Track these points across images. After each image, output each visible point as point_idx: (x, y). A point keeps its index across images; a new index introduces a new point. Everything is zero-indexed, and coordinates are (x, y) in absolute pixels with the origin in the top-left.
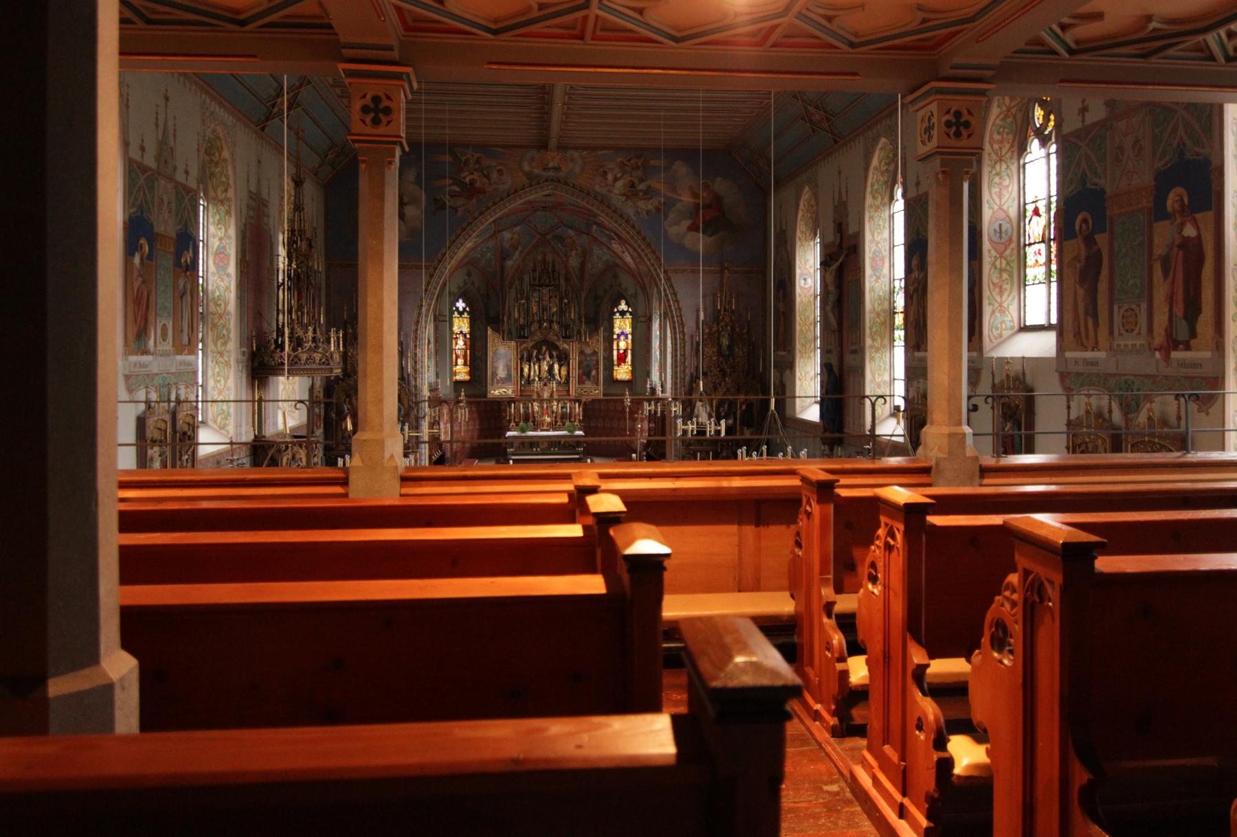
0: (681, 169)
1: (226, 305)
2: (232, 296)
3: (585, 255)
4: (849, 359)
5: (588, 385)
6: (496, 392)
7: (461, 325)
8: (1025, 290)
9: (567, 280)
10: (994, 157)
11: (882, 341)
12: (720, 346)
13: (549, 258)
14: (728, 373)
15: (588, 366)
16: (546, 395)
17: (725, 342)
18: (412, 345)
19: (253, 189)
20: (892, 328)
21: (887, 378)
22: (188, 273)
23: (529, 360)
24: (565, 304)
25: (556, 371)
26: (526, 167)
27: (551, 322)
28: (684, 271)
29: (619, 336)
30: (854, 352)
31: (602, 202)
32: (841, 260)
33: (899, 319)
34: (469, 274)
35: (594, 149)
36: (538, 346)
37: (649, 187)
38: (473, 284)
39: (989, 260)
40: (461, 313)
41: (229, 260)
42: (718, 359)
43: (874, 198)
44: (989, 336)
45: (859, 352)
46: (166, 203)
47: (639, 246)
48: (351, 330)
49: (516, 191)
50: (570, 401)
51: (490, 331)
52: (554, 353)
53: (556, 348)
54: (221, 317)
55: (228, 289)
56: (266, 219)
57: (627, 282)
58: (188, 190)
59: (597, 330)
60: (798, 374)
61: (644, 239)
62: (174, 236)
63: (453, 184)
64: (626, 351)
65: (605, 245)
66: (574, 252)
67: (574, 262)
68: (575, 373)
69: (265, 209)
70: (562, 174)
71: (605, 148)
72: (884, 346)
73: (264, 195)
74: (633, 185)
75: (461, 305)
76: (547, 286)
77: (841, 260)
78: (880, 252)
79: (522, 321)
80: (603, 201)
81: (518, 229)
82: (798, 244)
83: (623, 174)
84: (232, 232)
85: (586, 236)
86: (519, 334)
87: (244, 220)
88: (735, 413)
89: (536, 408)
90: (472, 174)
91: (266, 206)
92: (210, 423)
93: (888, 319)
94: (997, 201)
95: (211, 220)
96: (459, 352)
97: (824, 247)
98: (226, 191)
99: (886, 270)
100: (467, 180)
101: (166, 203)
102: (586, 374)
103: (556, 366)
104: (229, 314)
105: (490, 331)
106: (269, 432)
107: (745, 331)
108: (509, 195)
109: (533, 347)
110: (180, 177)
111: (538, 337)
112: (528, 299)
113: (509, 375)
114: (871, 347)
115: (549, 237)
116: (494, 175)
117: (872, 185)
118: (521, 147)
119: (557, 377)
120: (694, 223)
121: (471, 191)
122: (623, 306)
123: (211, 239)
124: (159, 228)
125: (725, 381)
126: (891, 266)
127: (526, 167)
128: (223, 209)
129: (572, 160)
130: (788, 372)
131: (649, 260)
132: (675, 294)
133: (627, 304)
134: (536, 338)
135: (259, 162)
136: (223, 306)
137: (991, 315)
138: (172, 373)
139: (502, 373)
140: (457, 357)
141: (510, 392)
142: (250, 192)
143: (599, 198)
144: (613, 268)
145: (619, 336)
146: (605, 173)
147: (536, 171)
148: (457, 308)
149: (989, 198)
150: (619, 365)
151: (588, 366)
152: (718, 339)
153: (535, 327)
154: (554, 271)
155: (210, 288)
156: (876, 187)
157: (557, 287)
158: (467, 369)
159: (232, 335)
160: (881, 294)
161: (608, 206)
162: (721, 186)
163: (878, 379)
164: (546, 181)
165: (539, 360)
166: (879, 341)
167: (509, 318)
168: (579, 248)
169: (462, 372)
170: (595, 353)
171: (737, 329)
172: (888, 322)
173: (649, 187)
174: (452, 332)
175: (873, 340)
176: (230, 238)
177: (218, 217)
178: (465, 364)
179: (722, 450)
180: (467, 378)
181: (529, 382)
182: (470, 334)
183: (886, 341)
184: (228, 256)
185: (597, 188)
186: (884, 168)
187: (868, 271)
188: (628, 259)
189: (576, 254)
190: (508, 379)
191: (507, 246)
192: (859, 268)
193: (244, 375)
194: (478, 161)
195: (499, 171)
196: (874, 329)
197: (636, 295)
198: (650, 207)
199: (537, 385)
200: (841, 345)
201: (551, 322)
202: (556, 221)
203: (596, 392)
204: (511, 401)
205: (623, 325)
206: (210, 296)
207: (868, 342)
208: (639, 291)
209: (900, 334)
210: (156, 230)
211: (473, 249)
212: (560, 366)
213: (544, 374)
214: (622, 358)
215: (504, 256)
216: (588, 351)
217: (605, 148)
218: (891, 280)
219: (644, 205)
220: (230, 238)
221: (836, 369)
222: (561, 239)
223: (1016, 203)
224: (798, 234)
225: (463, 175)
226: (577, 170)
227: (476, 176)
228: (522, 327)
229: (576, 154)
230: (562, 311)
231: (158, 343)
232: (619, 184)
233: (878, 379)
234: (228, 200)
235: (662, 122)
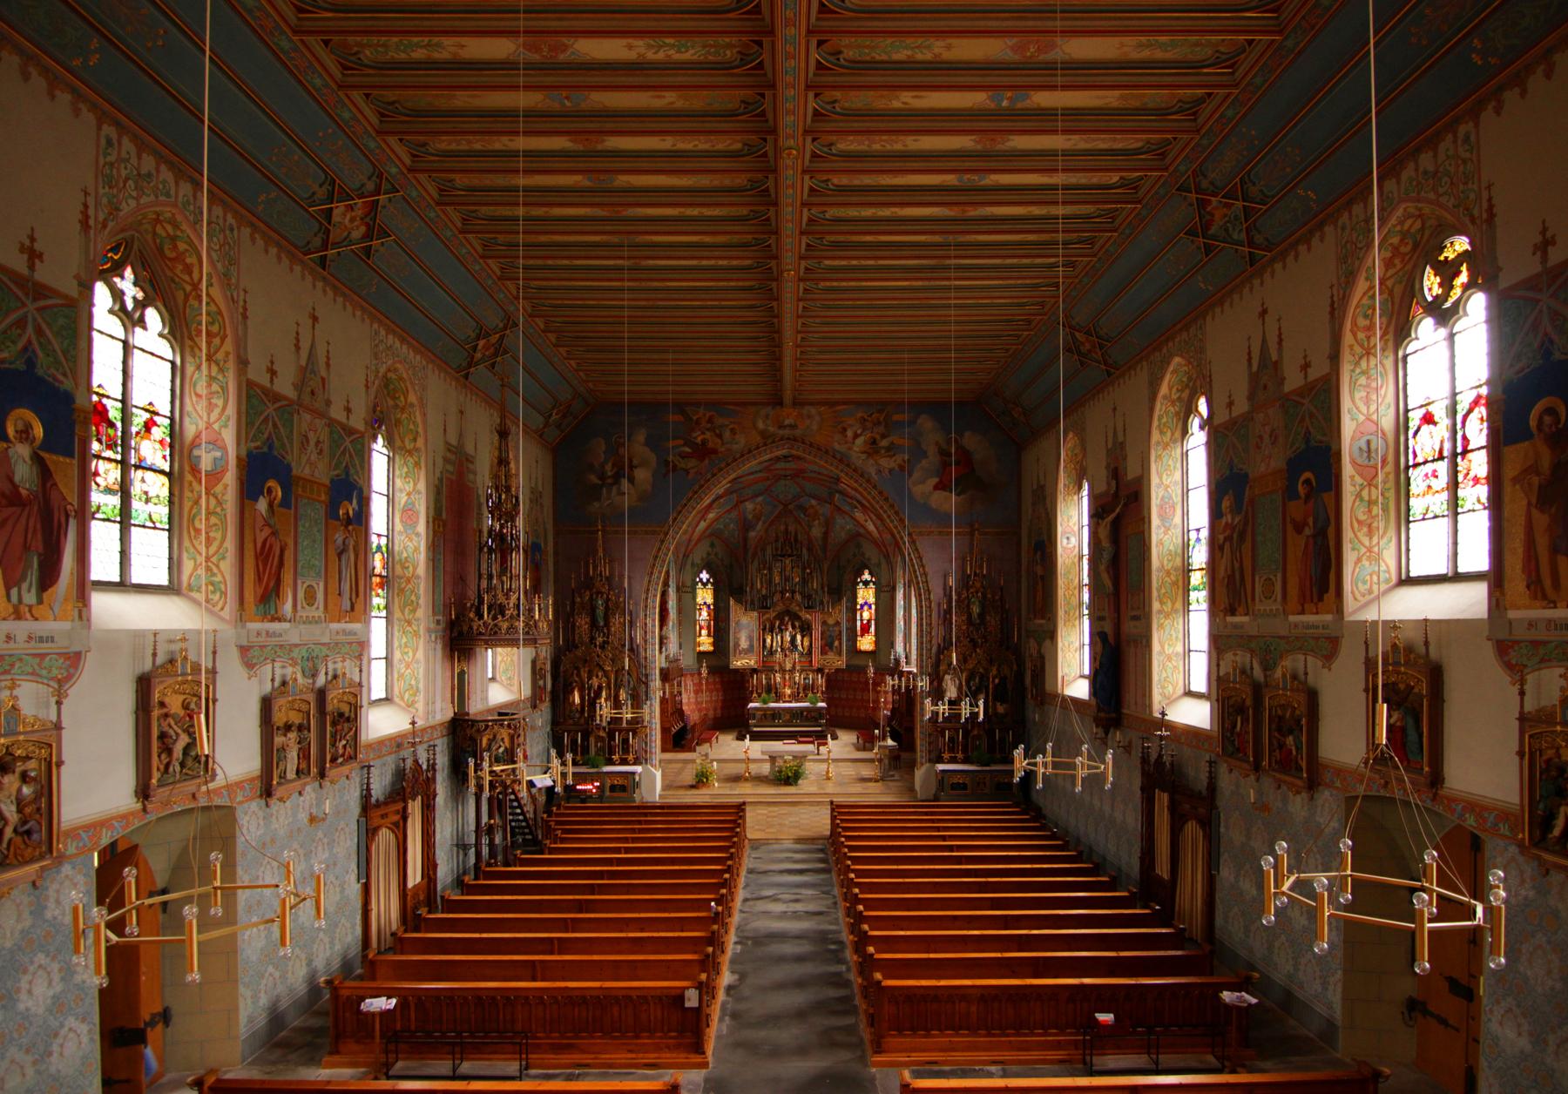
0: (926, 423)
1: (415, 568)
2: (422, 557)
3: (828, 525)
4: (1129, 627)
5: (831, 656)
6: (738, 663)
7: (705, 596)
8: (1408, 529)
9: (809, 550)
10: (1358, 350)
11: (1173, 604)
12: (970, 615)
13: (791, 528)
16: (788, 666)
17: (976, 609)
18: (642, 615)
19: (454, 442)
20: (1186, 590)
21: (1179, 648)
22: (350, 528)
23: (772, 631)
25: (799, 642)
26: (761, 425)
27: (793, 592)
28: (929, 533)
29: (862, 606)
30: (1136, 618)
31: (841, 461)
32: (1118, 510)
33: (1197, 578)
34: (712, 545)
35: (831, 404)
36: (780, 617)
37: (892, 443)
38: (716, 554)
39: (1352, 489)
40: (704, 585)
41: (418, 518)
43: (1162, 433)
44: (1353, 592)
45: (1143, 618)
46: (312, 443)
47: (882, 507)
48: (578, 600)
49: (750, 451)
50: (813, 671)
51: (732, 602)
52: (797, 624)
53: (799, 618)
54: (409, 581)
55: (416, 549)
56: (471, 477)
57: (871, 553)
58: (351, 431)
59: (840, 599)
60: (1060, 645)
61: (886, 499)
62: (327, 482)
63: (685, 445)
64: (869, 621)
67: (817, 532)
68: (817, 644)
69: (470, 466)
70: (798, 432)
71: (844, 403)
72: (1176, 611)
73: (470, 449)
74: (874, 442)
75: (704, 576)
77: (1118, 510)
78: (1171, 498)
79: (764, 592)
80: (843, 460)
81: (760, 499)
82: (1060, 498)
83: (864, 430)
84: (422, 486)
86: (762, 605)
87: (438, 474)
88: (987, 688)
89: (778, 679)
90: (703, 433)
91: (472, 462)
92: (397, 700)
93: (1180, 578)
94: (1364, 409)
95: (397, 473)
96: (703, 623)
97: (1093, 497)
98: (415, 440)
99: (1177, 520)
100: (699, 440)
101: (312, 443)
102: (827, 646)
103: (799, 637)
104: (418, 577)
105: (732, 602)
106: (475, 707)
108: (742, 456)
109: (775, 618)
110: (337, 413)
111: (780, 607)
112: (770, 569)
113: (751, 646)
114: (1160, 612)
115: (791, 507)
116: (727, 434)
117: (1159, 420)
118: (755, 404)
119: (800, 648)
120: (941, 482)
121: (703, 452)
122: (867, 576)
123: (398, 494)
124: (301, 469)
126: (1185, 514)
127: (761, 425)
128: (411, 461)
129: (809, 417)
130: (1048, 642)
132: (920, 558)
133: (870, 573)
134: (778, 608)
135: (462, 412)
136: (411, 569)
137: (1356, 564)
138: (324, 644)
139: (744, 644)
140: (701, 628)
141: (752, 663)
142: (447, 443)
143: (838, 456)
144: (857, 537)
145: (862, 606)
146: (845, 430)
147: (771, 429)
148: (701, 580)
149: (1351, 405)
150: (862, 636)
152: (968, 606)
153: (777, 597)
154: (796, 540)
155: (396, 548)
156: (1164, 420)
157: (800, 556)
158: (711, 640)
159: (421, 601)
160: (1172, 548)
161: (848, 465)
162: (971, 441)
163: (1168, 650)
164: (781, 439)
165: (781, 631)
166: (1169, 604)
167: (752, 588)
169: (705, 643)
170: (838, 624)
172: (1180, 583)
173: (892, 443)
174: (695, 604)
175: (1162, 603)
176: (419, 493)
177: (405, 470)
178: (709, 635)
180: (711, 648)
181: (772, 652)
182: (714, 604)
183: (1179, 605)
184: (417, 514)
185: (836, 446)
186: (1175, 397)
187: (1155, 521)
188: (871, 527)
190: (750, 650)
191: (750, 517)
192: (1143, 519)
193: (439, 646)
194: (710, 420)
195: (732, 430)
196: (1163, 591)
197: (879, 565)
198: (892, 465)
199: (779, 656)
200: (1118, 610)
201: (793, 592)
203: (840, 662)
204: (754, 671)
205: (866, 595)
206: (397, 558)
207: (1156, 606)
208: (883, 561)
209: (1199, 599)
210: (294, 472)
211: (716, 519)
212: (803, 637)
213: (787, 645)
214: (865, 629)
215: (746, 526)
216: (831, 621)
217: (844, 403)
218: (1186, 531)
219: (887, 463)
220: (419, 493)
221: (1111, 639)
222: (801, 508)
223: (1392, 410)
224: (1061, 486)
225: (694, 435)
226: (815, 427)
227: (708, 435)
228: (765, 598)
229: (813, 410)
230: (804, 581)
231: (299, 607)
232: (860, 441)
233: (1168, 650)
234: (417, 450)
235: (906, 387)
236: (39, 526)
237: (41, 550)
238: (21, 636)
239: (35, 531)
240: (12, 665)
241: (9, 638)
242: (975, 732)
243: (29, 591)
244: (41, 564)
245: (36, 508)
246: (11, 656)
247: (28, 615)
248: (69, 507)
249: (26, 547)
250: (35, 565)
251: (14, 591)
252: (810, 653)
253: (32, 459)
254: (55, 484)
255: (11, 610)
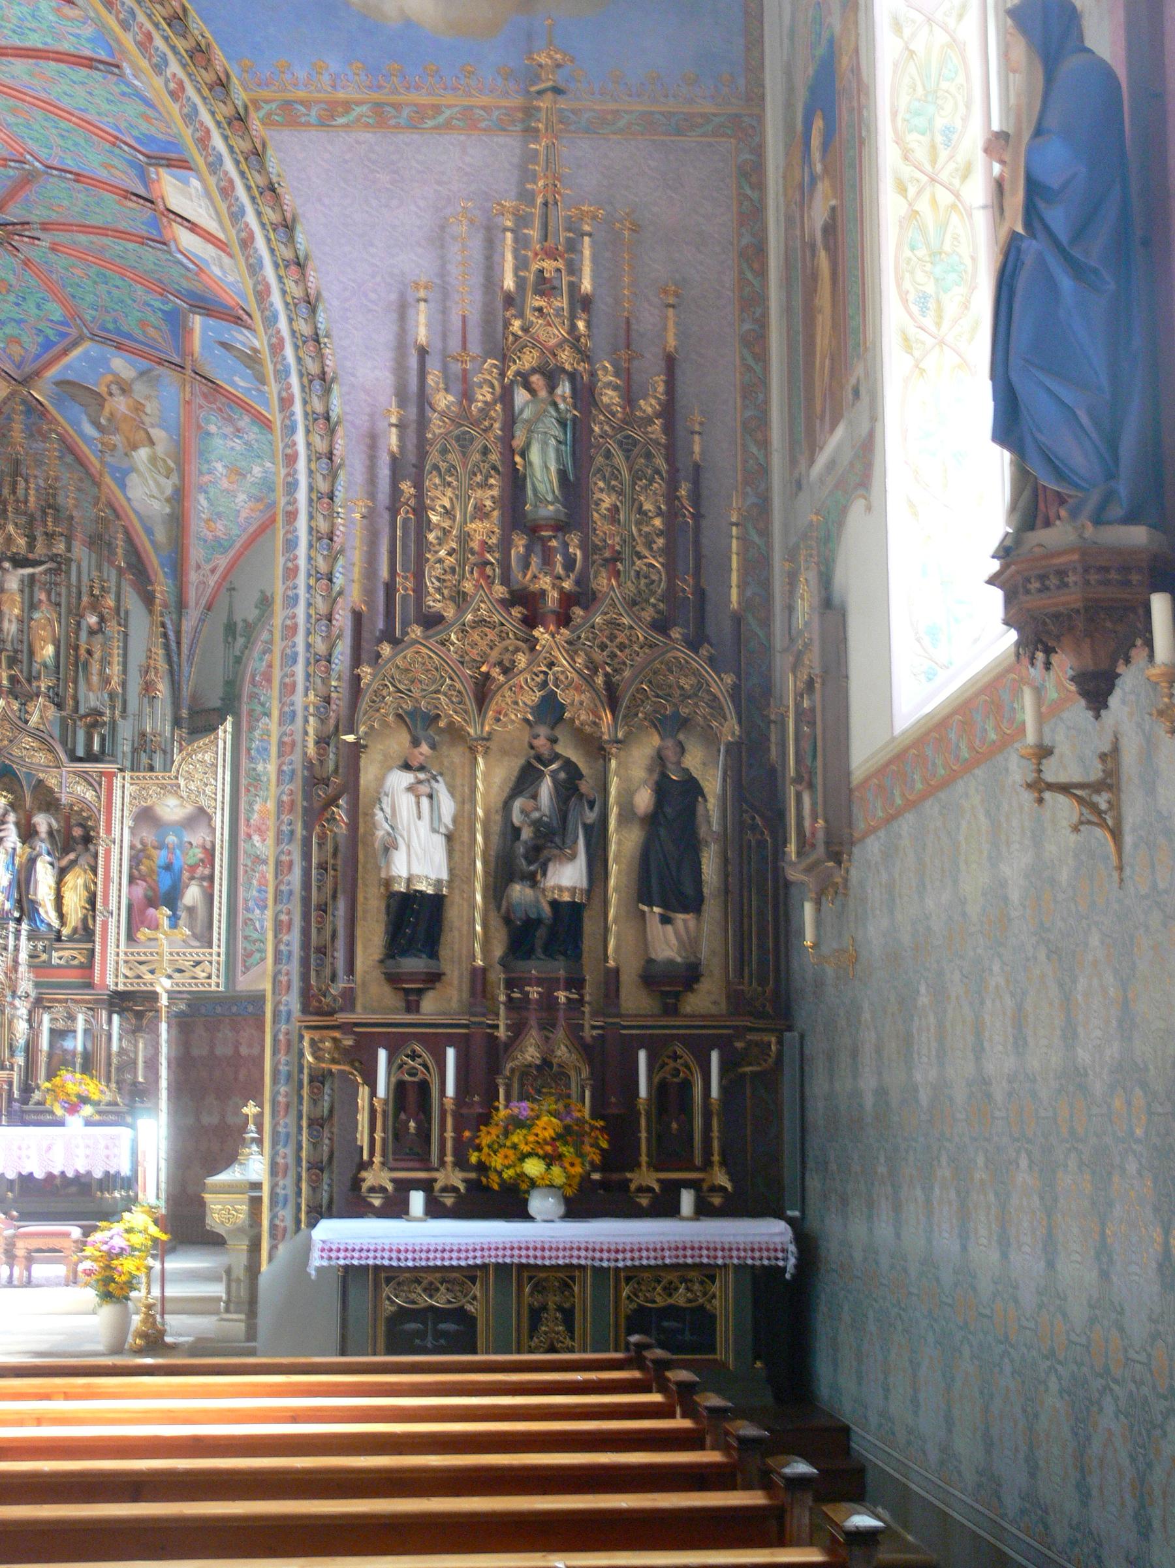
14: (553, 596)
15: (168, 867)
24: (92, 633)
42: (505, 544)
52: (42, 822)
53: (48, 801)
65: (246, 408)
66: (143, 454)
76: (19, 562)
85: (169, 377)
103: (44, 875)
107: (648, 406)
119: (48, 913)
125: (532, 643)
130: (857, 508)
131: (159, 68)
151: (168, 867)
157: (60, 564)
168: (156, 433)
170: (201, 816)
171: (610, 397)
179: (518, 1030)
189: (153, 459)
202: (56, 311)
212: (62, 873)
216: (172, 809)
242: (530, 1053)
252: (86, 933)
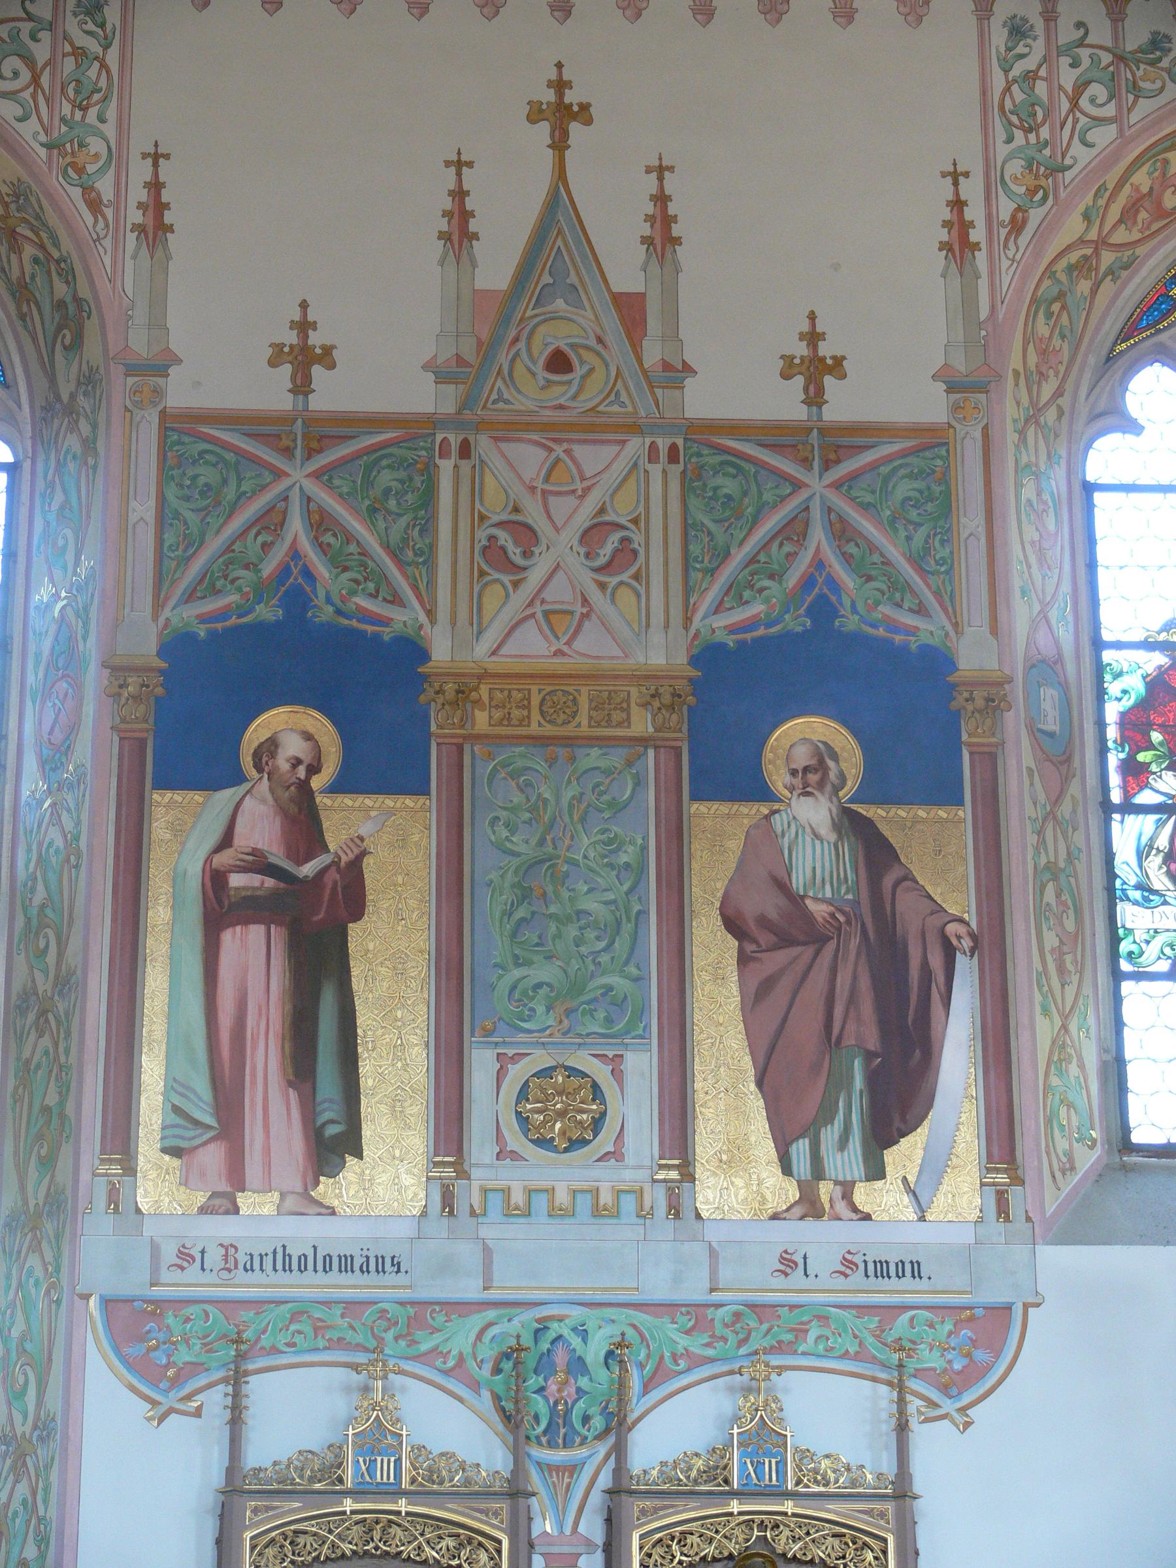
236: (865, 983)
237: (873, 1042)
238: (824, 1261)
239: (852, 1000)
240: (800, 1332)
241: (787, 1263)
243: (843, 1144)
244: (873, 1079)
245: (854, 943)
246: (792, 1307)
247: (841, 1207)
248: (951, 928)
249: (830, 1040)
250: (859, 1082)
251: (801, 1150)
253: (837, 827)
254: (908, 877)
255: (794, 1194)
